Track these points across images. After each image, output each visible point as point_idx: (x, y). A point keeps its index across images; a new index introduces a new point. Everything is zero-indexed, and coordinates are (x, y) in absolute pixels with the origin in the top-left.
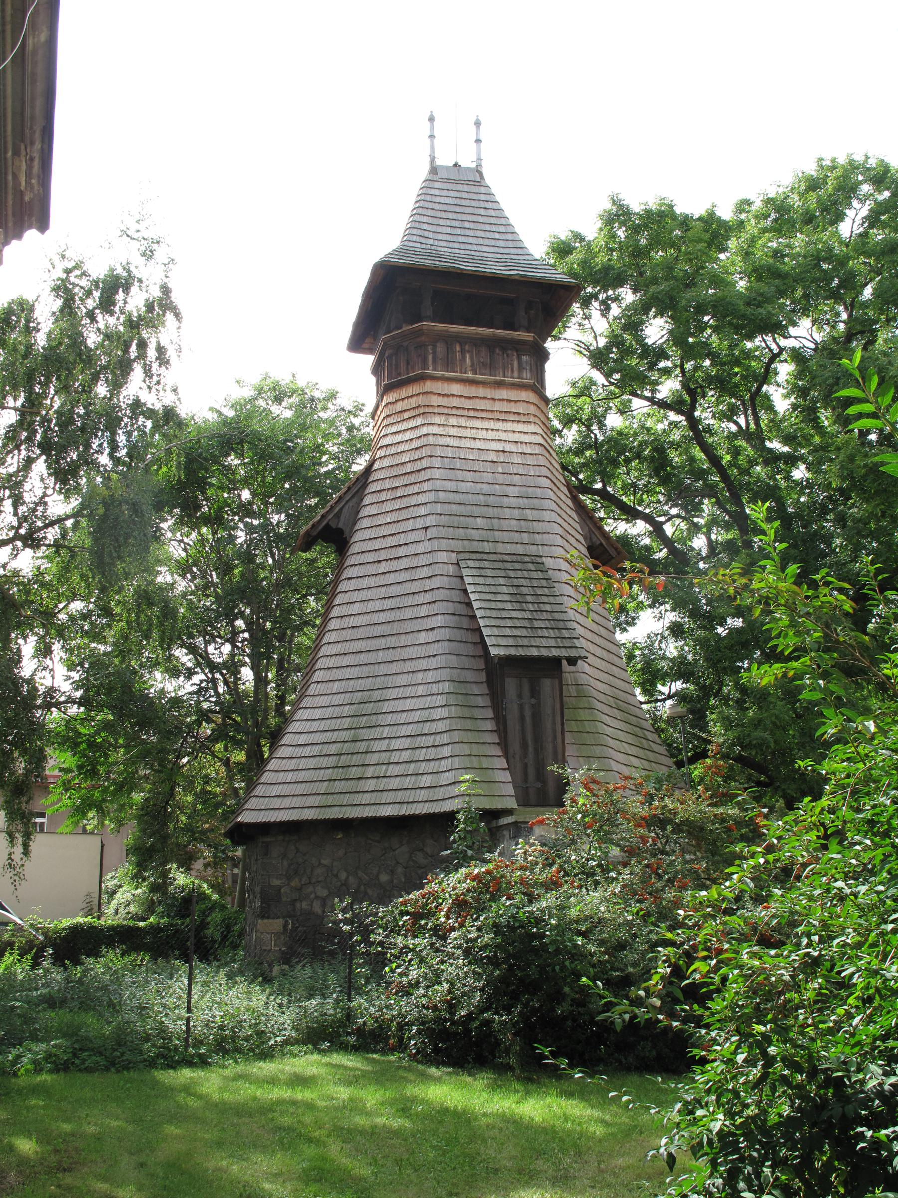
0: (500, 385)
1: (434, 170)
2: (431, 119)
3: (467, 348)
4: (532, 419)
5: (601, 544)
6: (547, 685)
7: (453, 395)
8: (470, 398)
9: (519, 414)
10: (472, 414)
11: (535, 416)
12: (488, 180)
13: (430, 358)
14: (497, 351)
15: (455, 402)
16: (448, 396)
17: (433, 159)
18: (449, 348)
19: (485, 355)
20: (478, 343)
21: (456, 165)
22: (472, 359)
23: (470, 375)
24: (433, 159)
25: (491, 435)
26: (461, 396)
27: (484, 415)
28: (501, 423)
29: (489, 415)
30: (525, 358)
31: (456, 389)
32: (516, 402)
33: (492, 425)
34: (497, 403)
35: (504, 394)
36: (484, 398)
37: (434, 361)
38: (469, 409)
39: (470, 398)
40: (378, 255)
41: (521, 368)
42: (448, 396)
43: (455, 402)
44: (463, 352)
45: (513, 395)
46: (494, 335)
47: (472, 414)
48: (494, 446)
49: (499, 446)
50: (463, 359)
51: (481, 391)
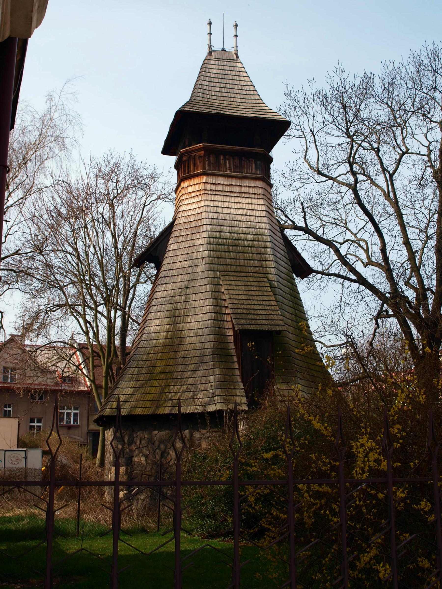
1: (210, 53)
3: (227, 157)
10: (228, 194)
12: (241, 58)
13: (207, 163)
16: (216, 184)
17: (210, 46)
21: (223, 50)
22: (229, 163)
23: (228, 172)
24: (210, 46)
25: (239, 206)
27: (236, 195)
30: (259, 162)
31: (220, 180)
32: (253, 187)
35: (247, 183)
36: (236, 185)
37: (209, 165)
40: (177, 109)
41: (256, 169)
42: (216, 184)
44: (225, 159)
47: (228, 194)
48: (240, 212)
49: (244, 212)
50: (225, 163)
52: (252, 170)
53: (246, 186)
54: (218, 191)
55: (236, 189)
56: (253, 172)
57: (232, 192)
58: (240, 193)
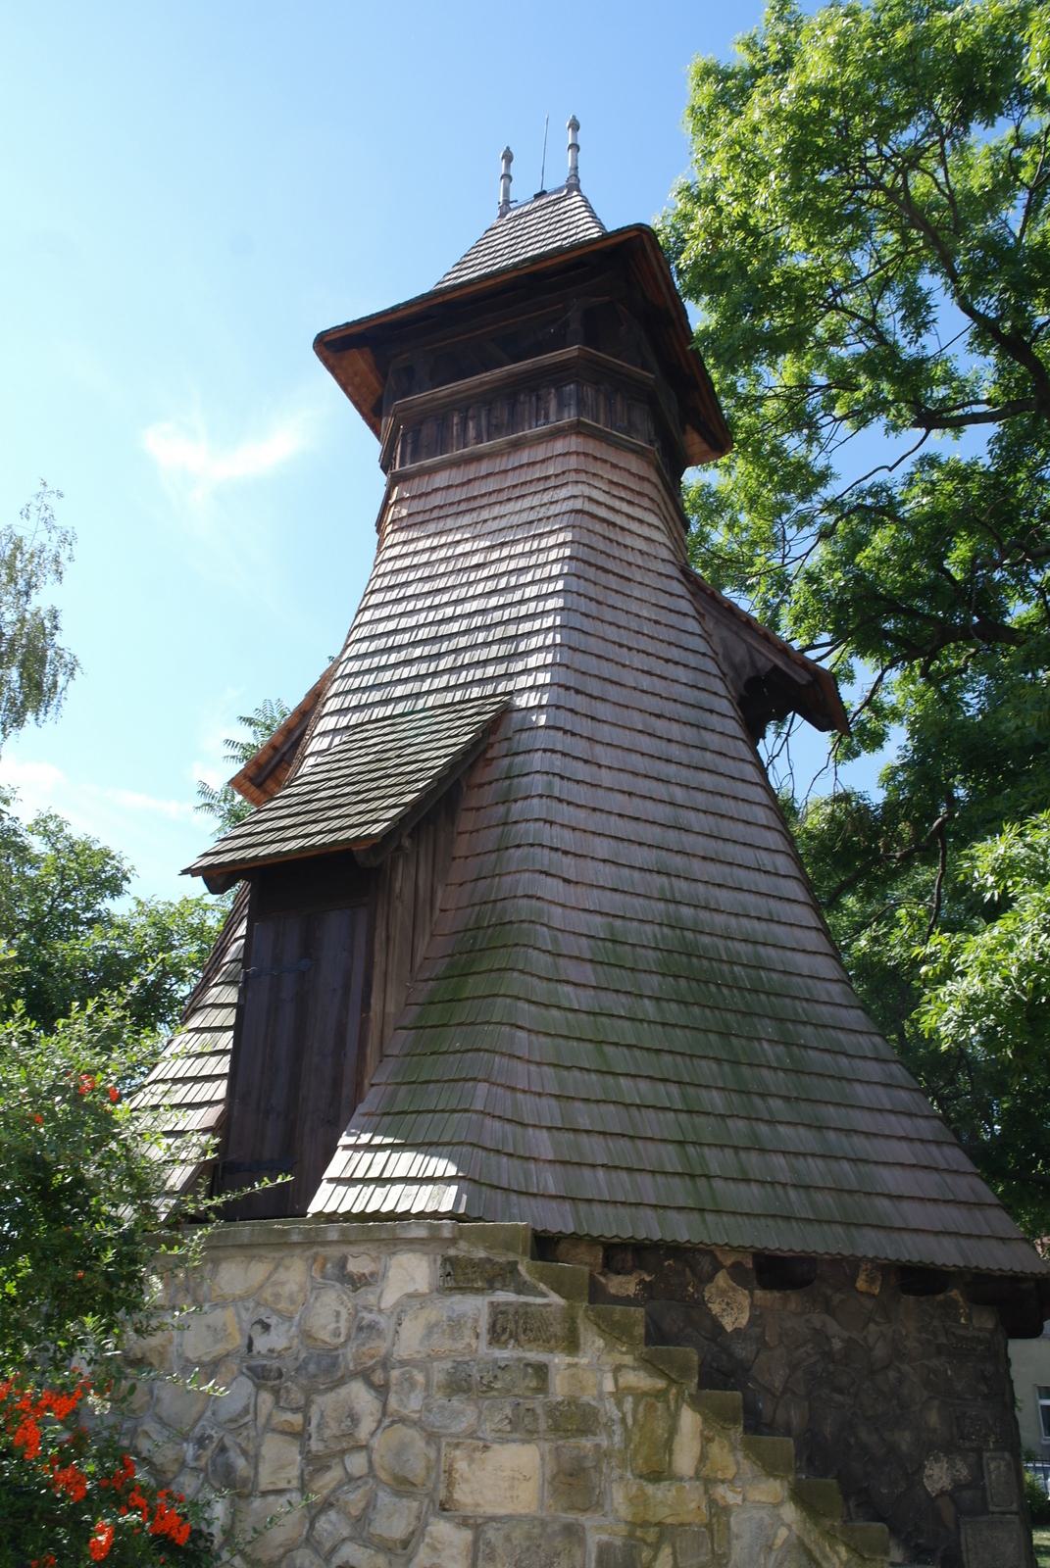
0: (516, 446)
2: (508, 157)
3: (471, 413)
4: (573, 477)
5: (776, 667)
6: (334, 925)
7: (436, 490)
8: (463, 484)
9: (547, 478)
10: (463, 507)
11: (577, 471)
14: (522, 398)
15: (437, 499)
16: (427, 494)
18: (444, 423)
19: (502, 413)
20: (486, 399)
26: (449, 487)
27: (485, 501)
28: (512, 503)
29: (493, 498)
31: (441, 479)
32: (543, 461)
33: (497, 511)
34: (510, 473)
35: (525, 456)
38: (459, 502)
39: (463, 484)
41: (562, 405)
42: (427, 494)
43: (437, 499)
45: (540, 452)
46: (510, 375)
47: (463, 507)
51: (485, 467)
52: (547, 417)
53: (521, 466)
54: (431, 510)
55: (491, 485)
56: (552, 418)
57: (475, 498)
58: (500, 491)
